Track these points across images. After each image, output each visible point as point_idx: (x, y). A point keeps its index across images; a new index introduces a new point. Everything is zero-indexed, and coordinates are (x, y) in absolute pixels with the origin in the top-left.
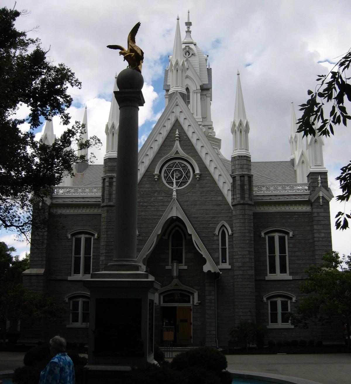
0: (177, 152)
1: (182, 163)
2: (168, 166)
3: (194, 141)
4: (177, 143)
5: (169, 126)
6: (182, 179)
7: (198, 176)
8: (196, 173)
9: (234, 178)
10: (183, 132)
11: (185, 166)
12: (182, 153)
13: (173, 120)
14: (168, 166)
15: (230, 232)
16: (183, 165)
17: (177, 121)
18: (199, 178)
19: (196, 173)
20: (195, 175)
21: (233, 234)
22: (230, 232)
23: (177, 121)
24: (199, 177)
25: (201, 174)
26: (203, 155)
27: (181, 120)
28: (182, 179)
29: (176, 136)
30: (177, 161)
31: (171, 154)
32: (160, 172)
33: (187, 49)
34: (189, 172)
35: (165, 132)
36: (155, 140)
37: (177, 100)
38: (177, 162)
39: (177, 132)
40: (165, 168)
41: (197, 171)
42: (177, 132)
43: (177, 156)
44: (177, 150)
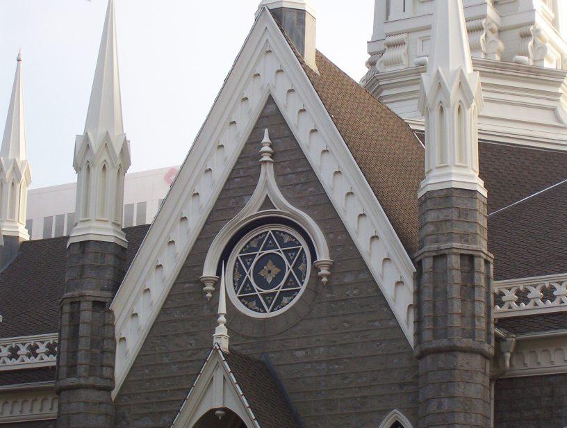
0: (267, 203)
1: (284, 233)
2: (248, 248)
3: (313, 157)
4: (267, 174)
5: (246, 121)
6: (282, 283)
7: (324, 271)
8: (318, 260)
9: (418, 264)
11: (294, 242)
12: (283, 204)
13: (256, 103)
14: (245, 247)
16: (287, 239)
17: (271, 100)
18: (328, 276)
19: (318, 260)
20: (316, 269)
24: (329, 273)
25: (334, 263)
26: (338, 199)
27: (280, 99)
28: (282, 283)
29: (263, 149)
30: (269, 229)
31: (251, 209)
34: (302, 259)
35: (233, 146)
36: (207, 171)
37: (267, 37)
38: (270, 230)
39: (266, 139)
40: (235, 254)
41: (323, 255)
42: (266, 139)
44: (267, 196)
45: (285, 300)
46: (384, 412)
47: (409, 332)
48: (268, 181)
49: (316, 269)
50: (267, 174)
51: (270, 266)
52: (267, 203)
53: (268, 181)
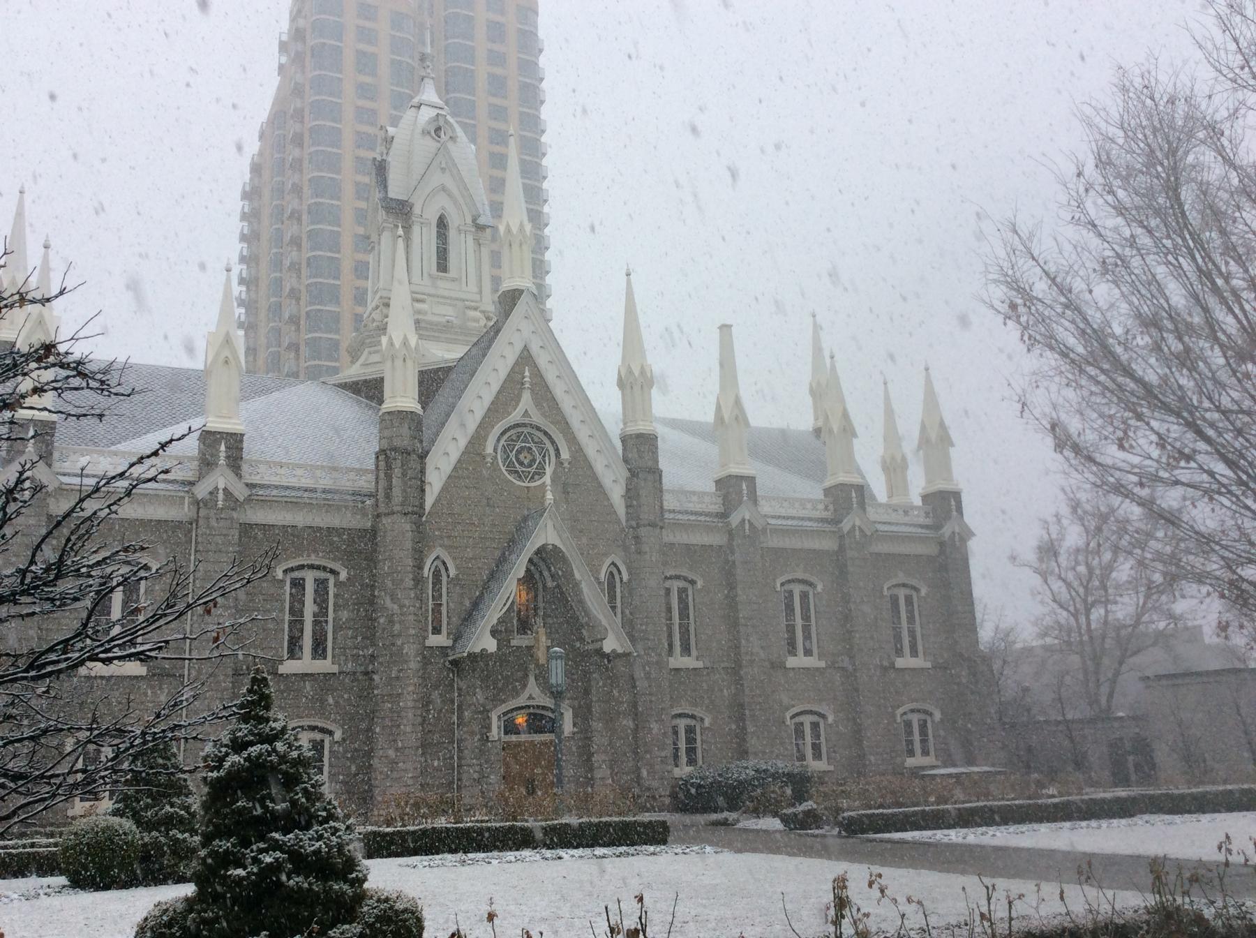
4: (526, 397)
10: (538, 374)
12: (537, 418)
13: (518, 348)
15: (625, 577)
17: (526, 348)
20: (560, 463)
21: (630, 581)
22: (625, 577)
23: (526, 348)
27: (535, 349)
30: (526, 430)
31: (515, 416)
32: (495, 450)
33: (441, 123)
39: (527, 374)
41: (565, 455)
43: (527, 421)
45: (536, 477)
46: (606, 555)
47: (621, 511)
48: (526, 399)
49: (560, 463)
50: (526, 397)
51: (525, 454)
52: (526, 413)
53: (526, 399)
